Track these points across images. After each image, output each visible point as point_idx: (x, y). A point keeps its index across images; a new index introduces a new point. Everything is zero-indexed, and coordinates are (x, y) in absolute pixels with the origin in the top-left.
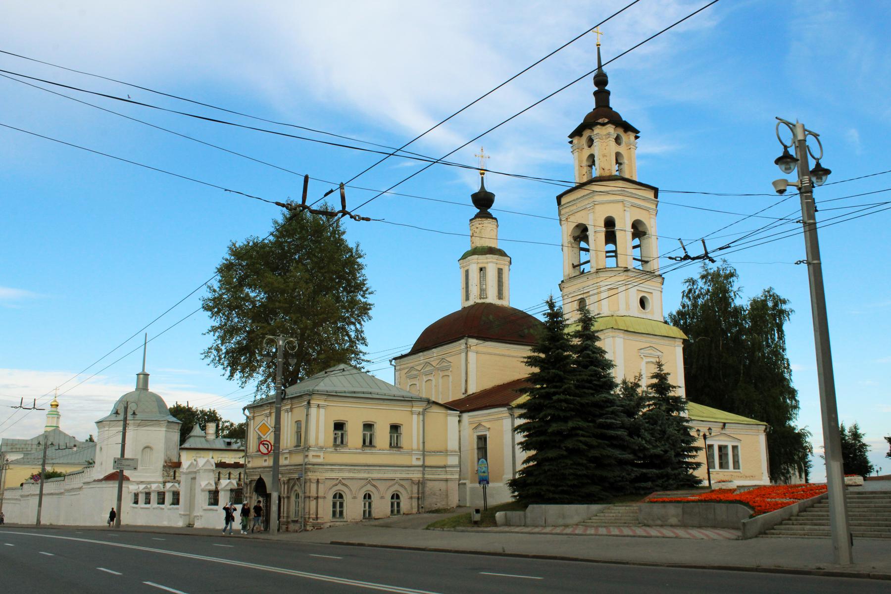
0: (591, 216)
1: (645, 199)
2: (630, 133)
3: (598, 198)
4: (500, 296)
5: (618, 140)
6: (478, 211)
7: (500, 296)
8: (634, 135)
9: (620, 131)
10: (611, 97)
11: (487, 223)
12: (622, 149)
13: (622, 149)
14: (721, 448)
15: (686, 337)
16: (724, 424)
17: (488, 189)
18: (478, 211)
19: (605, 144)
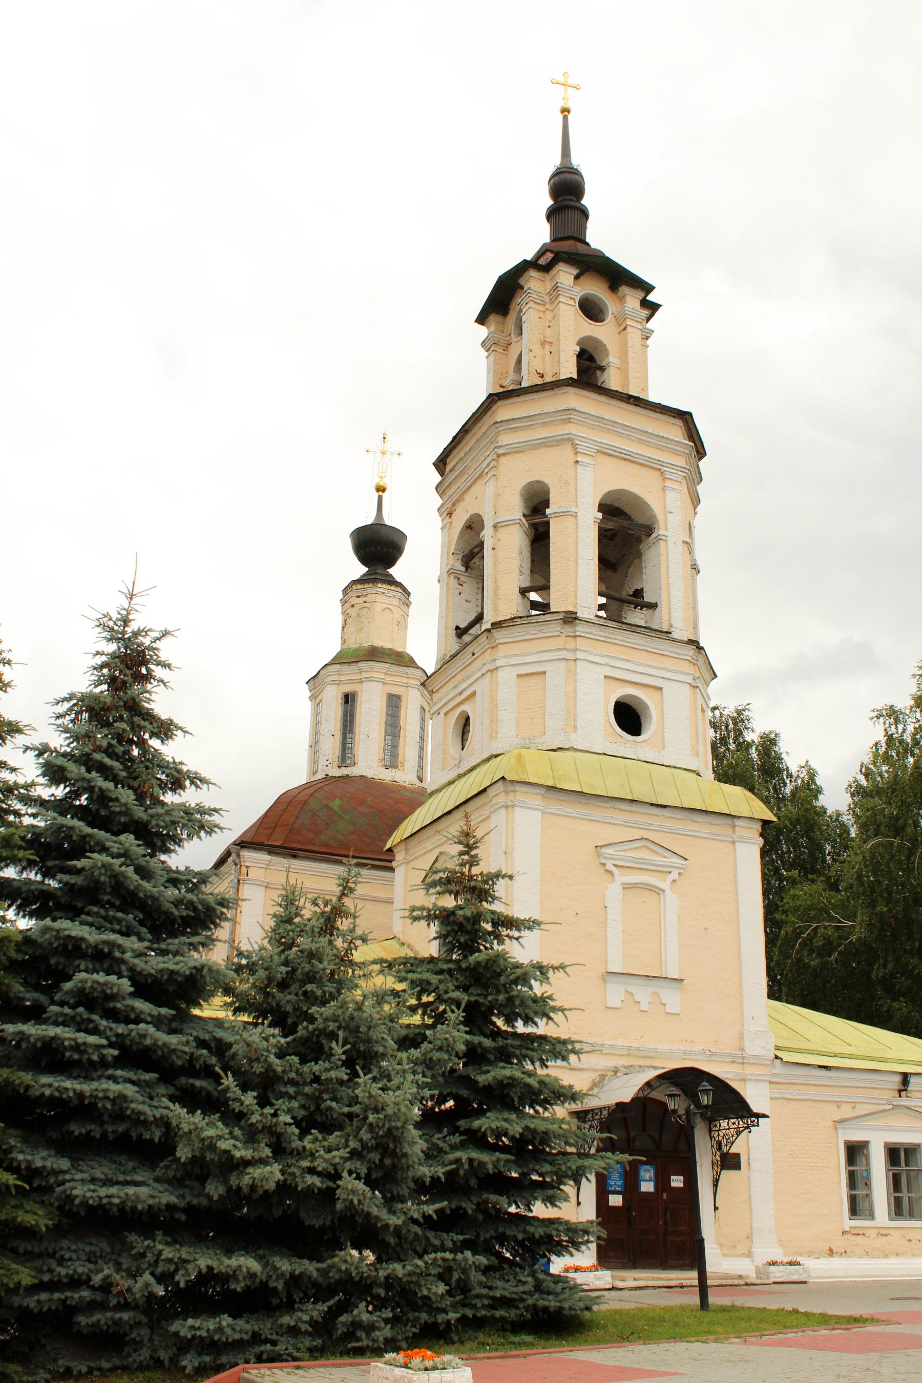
0: (490, 489)
1: (662, 443)
2: (624, 290)
3: (506, 439)
4: (392, 760)
5: (591, 310)
6: (367, 569)
7: (392, 760)
8: (641, 295)
9: (595, 288)
10: (590, 224)
11: (380, 595)
12: (602, 332)
13: (602, 332)
14: (894, 1153)
15: (769, 816)
16: (905, 1078)
17: (390, 520)
18: (365, 569)
19: (549, 315)
